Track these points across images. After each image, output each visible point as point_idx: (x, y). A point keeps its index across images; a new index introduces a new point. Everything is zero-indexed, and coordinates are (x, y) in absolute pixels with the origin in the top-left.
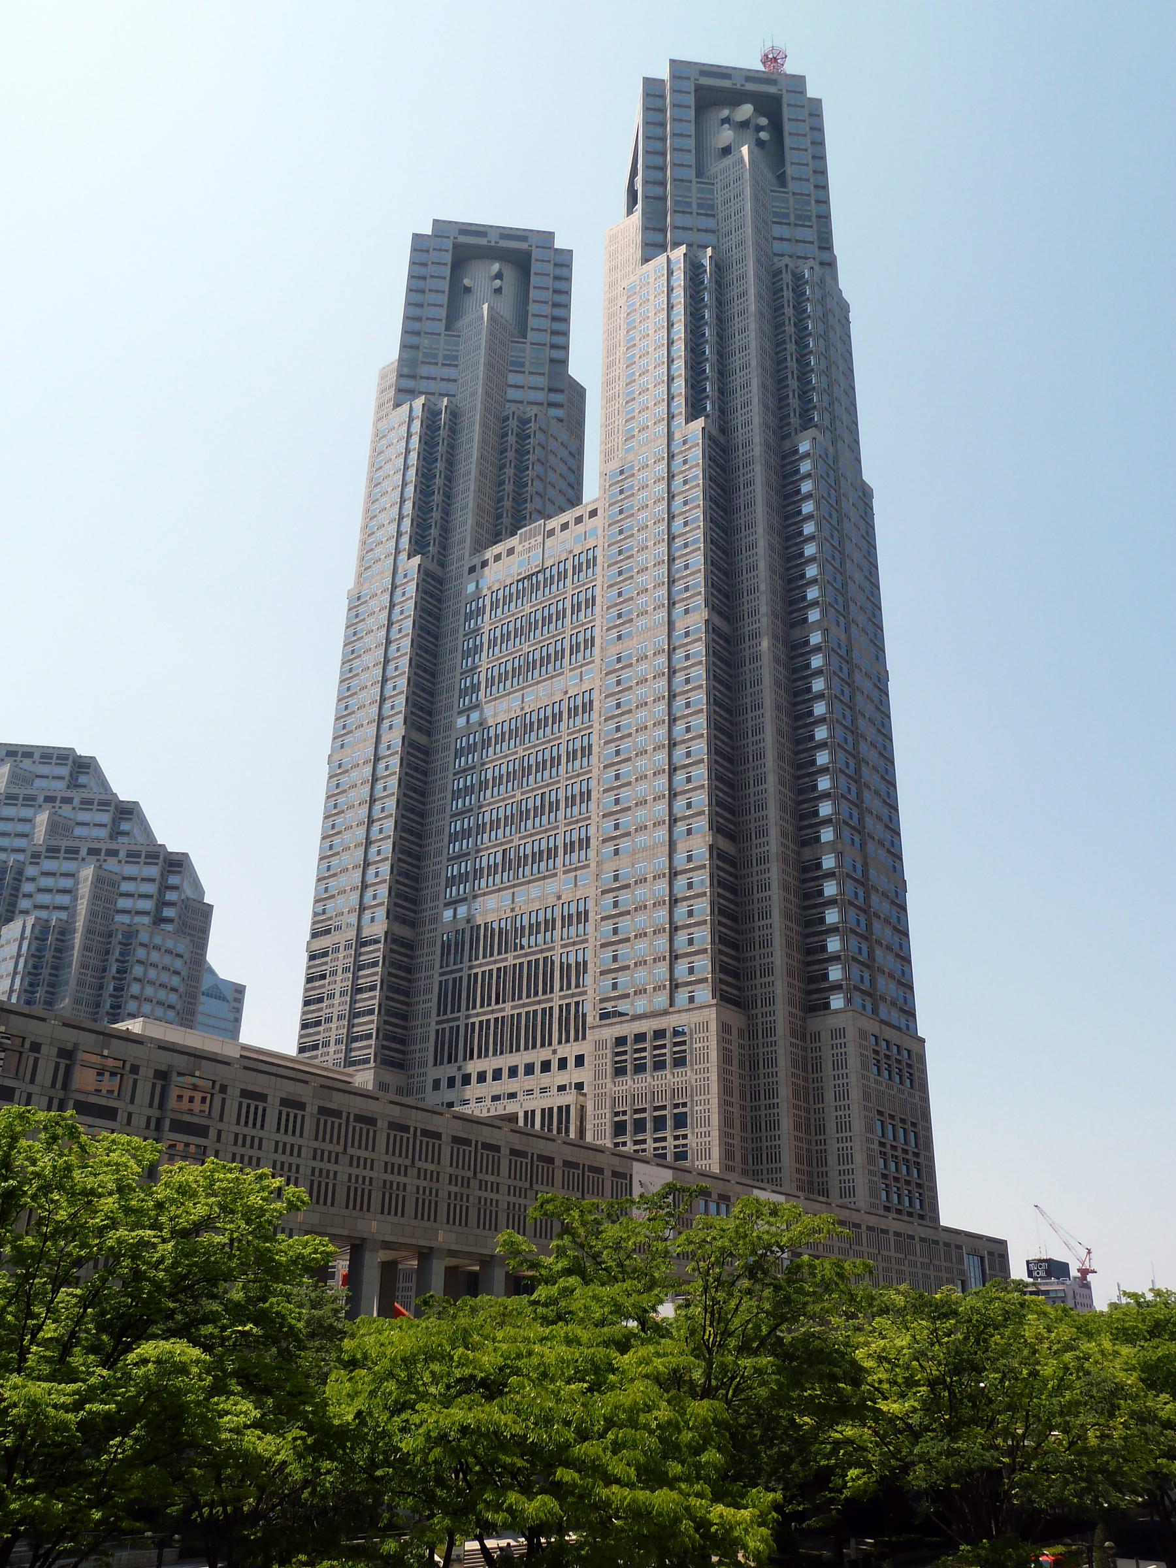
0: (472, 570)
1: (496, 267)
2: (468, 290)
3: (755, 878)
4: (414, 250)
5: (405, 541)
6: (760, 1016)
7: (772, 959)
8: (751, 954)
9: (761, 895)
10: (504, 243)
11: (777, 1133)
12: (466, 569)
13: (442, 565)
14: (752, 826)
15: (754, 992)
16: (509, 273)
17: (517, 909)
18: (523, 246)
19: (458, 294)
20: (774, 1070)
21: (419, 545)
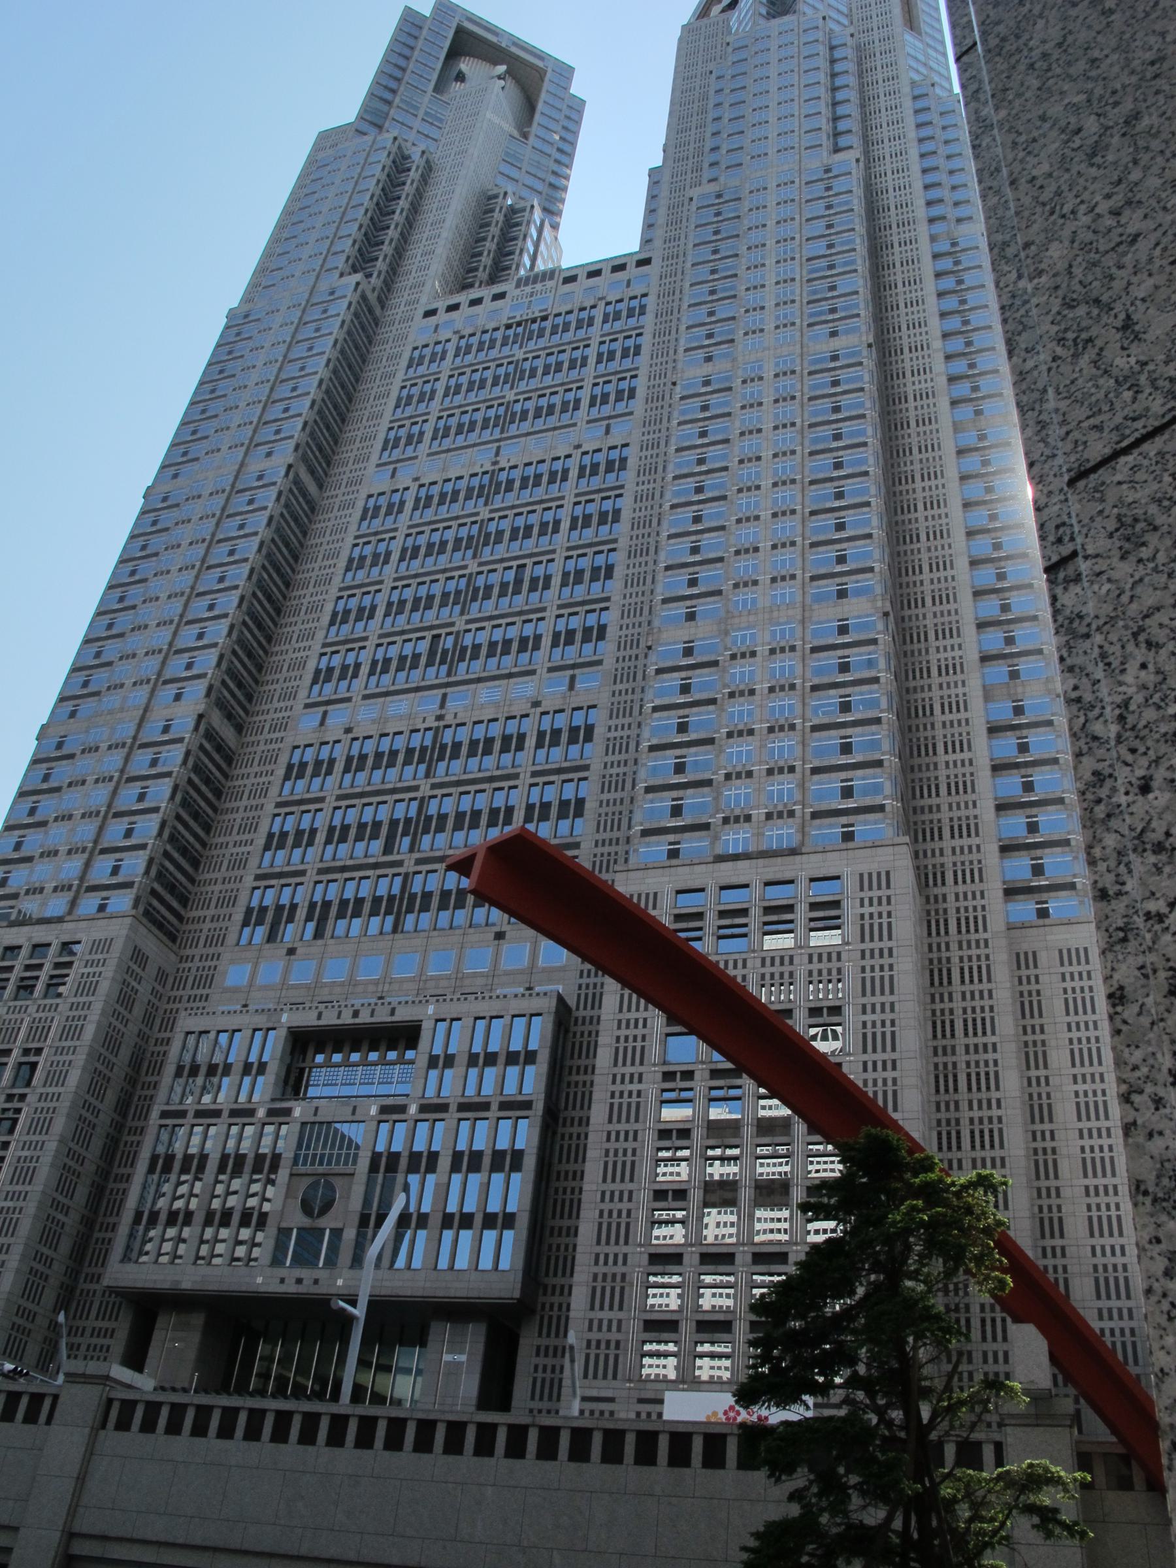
0: (430, 313)
1: (502, 69)
2: (461, 77)
5: (340, 262)
7: (977, 812)
8: (927, 802)
9: (948, 717)
10: (514, 49)
11: (994, 1095)
12: (421, 312)
13: (382, 303)
14: (929, 622)
15: (938, 860)
17: (449, 719)
18: (540, 64)
19: (449, 75)
20: (985, 986)
21: (362, 261)
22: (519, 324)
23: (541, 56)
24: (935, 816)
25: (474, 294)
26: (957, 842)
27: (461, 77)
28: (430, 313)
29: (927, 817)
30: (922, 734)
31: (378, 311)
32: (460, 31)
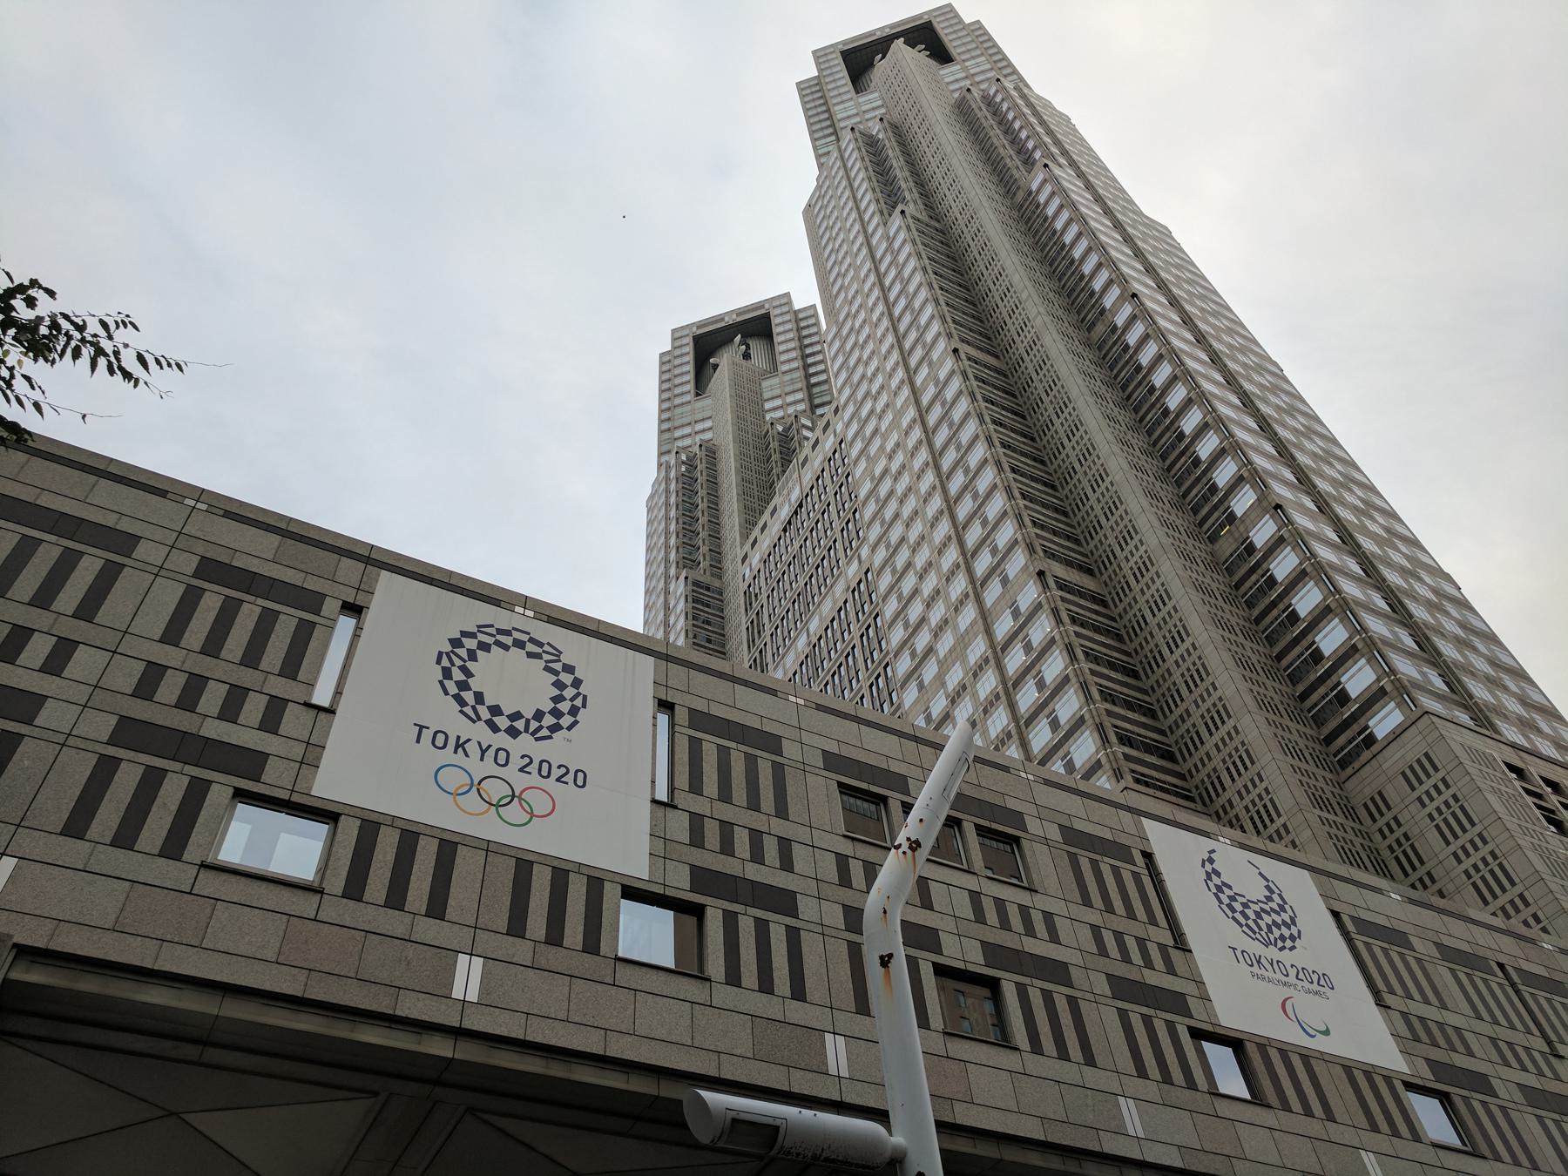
0: (743, 561)
3: (1141, 600)
4: (662, 363)
5: (673, 571)
6: (1236, 800)
7: (1219, 693)
8: (1177, 712)
14: (1112, 540)
16: (757, 347)
22: (789, 523)
23: (760, 305)
24: (1189, 724)
25: (761, 524)
26: (1217, 737)
27: (716, 366)
28: (743, 561)
29: (1183, 728)
30: (1147, 649)
31: (716, 583)
32: (698, 340)
